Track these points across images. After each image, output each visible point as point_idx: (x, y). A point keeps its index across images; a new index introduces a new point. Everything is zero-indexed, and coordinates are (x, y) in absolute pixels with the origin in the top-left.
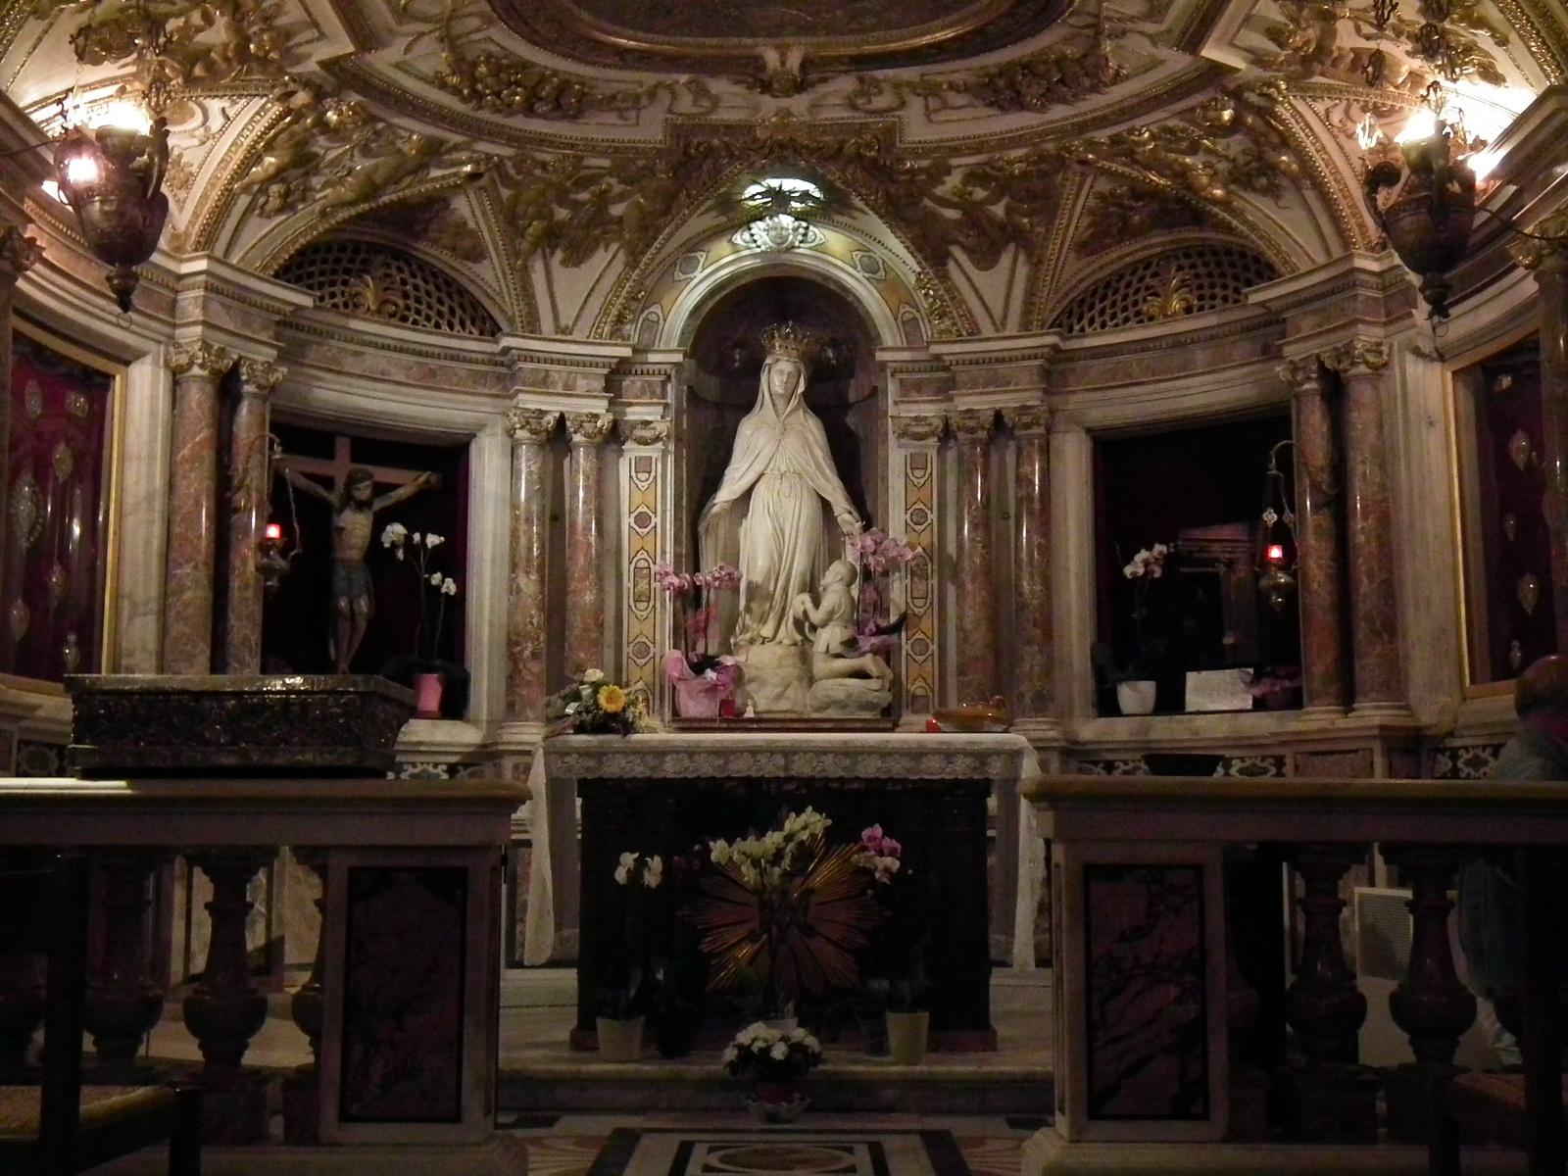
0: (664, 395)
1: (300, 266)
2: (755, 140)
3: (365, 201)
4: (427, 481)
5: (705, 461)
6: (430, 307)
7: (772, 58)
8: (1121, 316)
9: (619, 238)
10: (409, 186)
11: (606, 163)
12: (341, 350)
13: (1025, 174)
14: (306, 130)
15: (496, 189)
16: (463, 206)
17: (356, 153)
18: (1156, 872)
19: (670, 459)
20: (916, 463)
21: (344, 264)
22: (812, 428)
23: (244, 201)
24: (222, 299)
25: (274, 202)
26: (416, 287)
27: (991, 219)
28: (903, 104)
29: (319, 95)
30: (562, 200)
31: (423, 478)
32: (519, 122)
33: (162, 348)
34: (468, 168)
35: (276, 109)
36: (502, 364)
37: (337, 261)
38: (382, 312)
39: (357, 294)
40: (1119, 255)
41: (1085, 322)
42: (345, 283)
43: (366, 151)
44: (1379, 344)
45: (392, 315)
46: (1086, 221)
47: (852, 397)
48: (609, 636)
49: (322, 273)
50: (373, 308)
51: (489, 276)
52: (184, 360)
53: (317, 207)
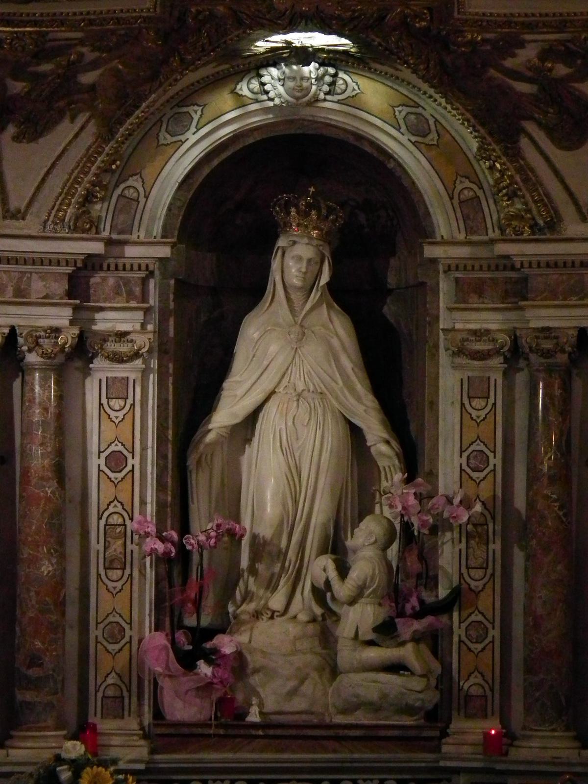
0: (144, 298)
5: (197, 369)
19: (153, 379)
20: (475, 389)
22: (339, 329)
47: (392, 280)
48: (72, 612)
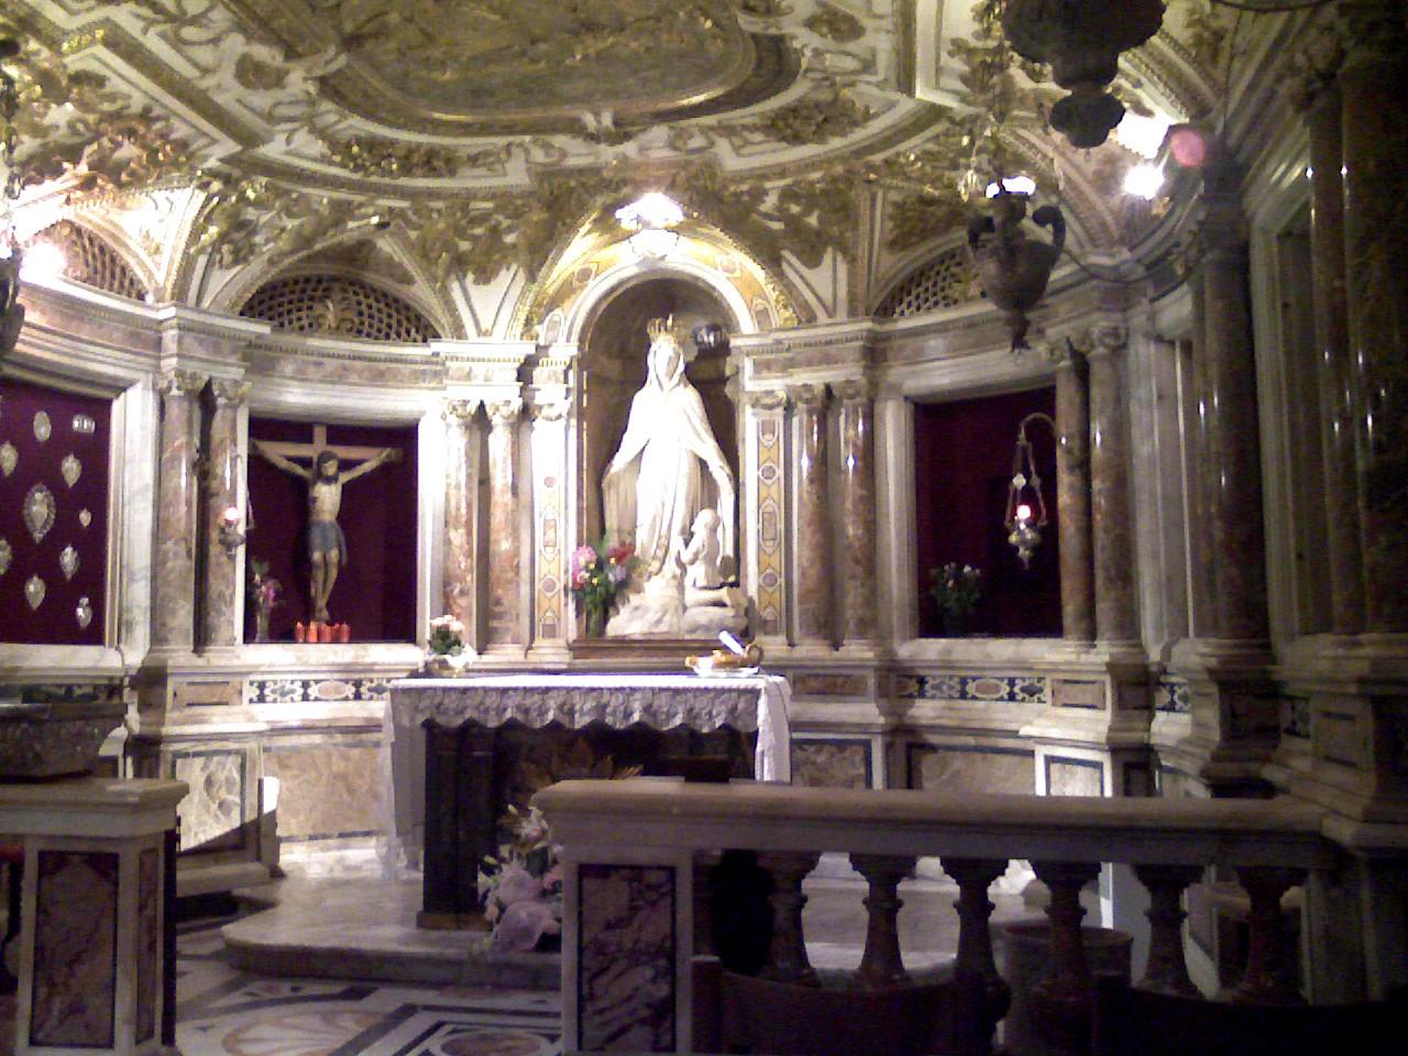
0: (566, 382)
1: (261, 303)
2: (603, 179)
3: (302, 249)
4: (388, 456)
5: (605, 429)
6: (381, 321)
7: (589, 119)
8: (932, 300)
9: (516, 260)
10: (333, 236)
11: (489, 205)
12: (304, 362)
13: (823, 192)
14: (233, 205)
15: (405, 233)
16: (386, 245)
17: (283, 215)
18: (636, 871)
19: (573, 432)
20: (766, 428)
21: (309, 292)
22: (690, 398)
23: (202, 260)
24: (194, 334)
25: (228, 258)
26: (370, 307)
27: (808, 226)
28: (712, 144)
29: (227, 180)
30: (463, 236)
31: (384, 455)
32: (403, 181)
33: (151, 375)
34: (375, 220)
35: (201, 196)
36: (437, 363)
37: (303, 291)
38: (337, 331)
39: (321, 316)
40: (922, 253)
41: (904, 305)
42: (310, 308)
43: (290, 215)
44: (1116, 329)
45: (350, 330)
46: (890, 225)
47: (728, 372)
48: (525, 573)
49: (290, 302)
50: (334, 325)
51: (421, 293)
52: (165, 385)
53: (266, 257)
